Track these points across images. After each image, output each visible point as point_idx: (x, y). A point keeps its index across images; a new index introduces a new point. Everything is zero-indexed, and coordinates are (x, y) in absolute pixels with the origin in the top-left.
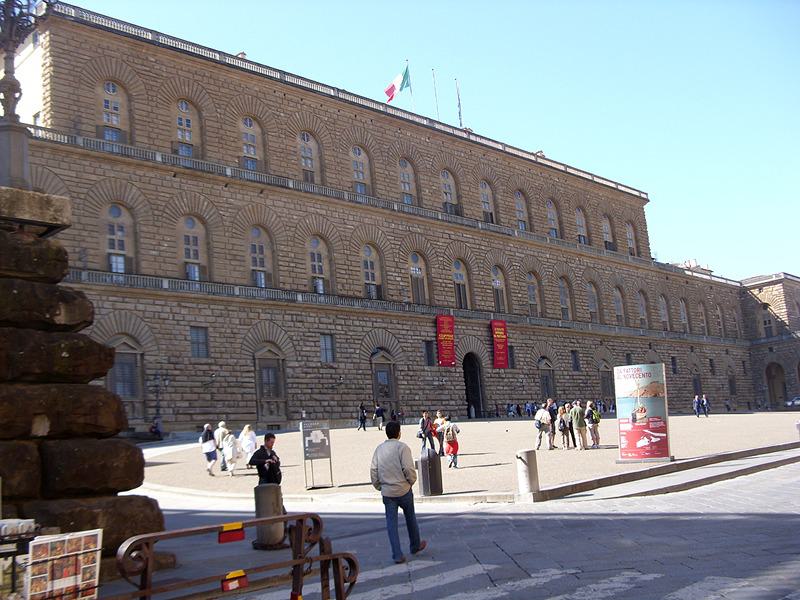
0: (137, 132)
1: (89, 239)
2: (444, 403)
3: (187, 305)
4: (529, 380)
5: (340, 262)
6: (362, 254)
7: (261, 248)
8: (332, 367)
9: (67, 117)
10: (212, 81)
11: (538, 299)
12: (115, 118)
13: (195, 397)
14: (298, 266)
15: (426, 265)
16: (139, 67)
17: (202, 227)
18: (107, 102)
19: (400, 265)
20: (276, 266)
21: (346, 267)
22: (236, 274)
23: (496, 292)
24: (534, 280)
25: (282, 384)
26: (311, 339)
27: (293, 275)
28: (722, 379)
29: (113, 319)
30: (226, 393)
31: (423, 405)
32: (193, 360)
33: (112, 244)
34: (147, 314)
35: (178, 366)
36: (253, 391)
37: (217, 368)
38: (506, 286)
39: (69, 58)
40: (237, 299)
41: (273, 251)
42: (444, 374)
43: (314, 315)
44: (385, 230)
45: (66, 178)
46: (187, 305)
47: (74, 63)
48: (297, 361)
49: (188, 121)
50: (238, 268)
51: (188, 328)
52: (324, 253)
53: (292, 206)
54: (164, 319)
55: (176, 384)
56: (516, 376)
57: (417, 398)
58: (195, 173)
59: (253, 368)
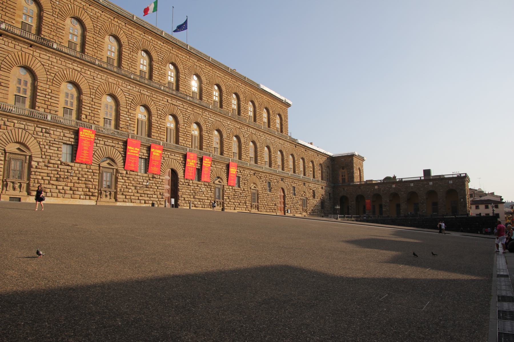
2: (149, 196)
4: (207, 189)
5: (86, 101)
8: (69, 165)
14: (53, 98)
21: (91, 105)
26: (54, 145)
27: (47, 103)
31: (134, 196)
42: (151, 179)
43: (61, 131)
48: (42, 158)
52: (75, 94)
53: (55, 61)
57: (130, 191)
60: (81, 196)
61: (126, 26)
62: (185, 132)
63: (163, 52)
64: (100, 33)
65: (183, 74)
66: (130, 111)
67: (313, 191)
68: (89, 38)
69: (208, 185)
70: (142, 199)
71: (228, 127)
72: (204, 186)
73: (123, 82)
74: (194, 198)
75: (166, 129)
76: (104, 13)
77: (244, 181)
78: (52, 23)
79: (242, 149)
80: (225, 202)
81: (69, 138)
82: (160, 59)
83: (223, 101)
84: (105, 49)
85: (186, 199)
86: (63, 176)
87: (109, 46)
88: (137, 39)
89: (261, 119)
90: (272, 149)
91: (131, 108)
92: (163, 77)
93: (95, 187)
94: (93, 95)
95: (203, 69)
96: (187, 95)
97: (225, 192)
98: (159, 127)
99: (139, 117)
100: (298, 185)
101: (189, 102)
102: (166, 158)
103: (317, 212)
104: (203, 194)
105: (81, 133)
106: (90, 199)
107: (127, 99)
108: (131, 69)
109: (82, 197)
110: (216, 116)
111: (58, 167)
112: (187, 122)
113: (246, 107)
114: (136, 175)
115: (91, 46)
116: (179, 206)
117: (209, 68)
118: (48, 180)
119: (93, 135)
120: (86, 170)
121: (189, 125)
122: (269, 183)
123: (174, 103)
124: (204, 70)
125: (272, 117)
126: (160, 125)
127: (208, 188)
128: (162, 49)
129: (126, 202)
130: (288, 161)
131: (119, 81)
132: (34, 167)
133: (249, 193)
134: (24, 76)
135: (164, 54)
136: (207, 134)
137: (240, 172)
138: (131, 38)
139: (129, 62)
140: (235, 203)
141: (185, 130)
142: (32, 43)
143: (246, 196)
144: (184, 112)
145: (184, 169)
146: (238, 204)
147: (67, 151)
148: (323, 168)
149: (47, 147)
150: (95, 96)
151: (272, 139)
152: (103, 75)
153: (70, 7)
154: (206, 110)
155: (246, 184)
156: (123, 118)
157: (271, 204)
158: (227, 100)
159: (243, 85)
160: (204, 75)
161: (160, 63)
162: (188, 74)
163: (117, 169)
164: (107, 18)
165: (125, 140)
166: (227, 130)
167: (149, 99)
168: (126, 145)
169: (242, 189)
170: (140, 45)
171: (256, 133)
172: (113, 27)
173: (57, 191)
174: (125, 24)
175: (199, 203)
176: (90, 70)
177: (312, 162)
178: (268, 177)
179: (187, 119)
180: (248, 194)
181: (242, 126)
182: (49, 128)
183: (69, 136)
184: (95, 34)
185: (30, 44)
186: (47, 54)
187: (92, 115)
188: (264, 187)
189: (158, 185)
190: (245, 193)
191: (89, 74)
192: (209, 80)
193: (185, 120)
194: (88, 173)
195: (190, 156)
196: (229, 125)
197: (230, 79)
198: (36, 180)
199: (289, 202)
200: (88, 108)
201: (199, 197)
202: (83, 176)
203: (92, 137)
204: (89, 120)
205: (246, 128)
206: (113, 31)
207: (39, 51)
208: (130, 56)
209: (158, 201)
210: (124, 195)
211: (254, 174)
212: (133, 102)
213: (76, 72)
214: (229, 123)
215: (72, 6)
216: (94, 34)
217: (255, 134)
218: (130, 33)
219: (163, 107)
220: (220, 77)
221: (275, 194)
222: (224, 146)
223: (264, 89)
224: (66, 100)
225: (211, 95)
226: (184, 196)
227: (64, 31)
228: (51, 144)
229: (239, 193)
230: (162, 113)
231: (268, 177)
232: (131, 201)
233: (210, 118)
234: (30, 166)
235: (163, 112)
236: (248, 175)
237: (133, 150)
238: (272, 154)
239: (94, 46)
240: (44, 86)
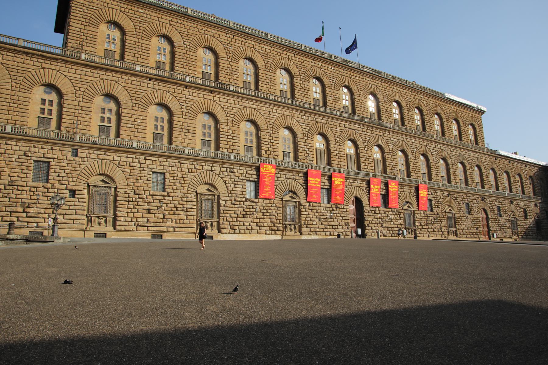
1: (84, 116)
2: (334, 227)
4: (396, 216)
8: (253, 202)
10: (182, 26)
14: (234, 138)
16: (132, 15)
18: (109, 35)
21: (269, 141)
22: (187, 141)
26: (239, 183)
27: (229, 143)
30: (174, 214)
31: (318, 228)
33: (103, 119)
39: (84, 8)
42: (335, 209)
44: (298, 119)
45: (72, 78)
47: (86, 11)
48: (228, 196)
50: (190, 138)
52: (254, 131)
53: (233, 102)
56: (387, 213)
57: (314, 223)
59: (195, 200)
60: (267, 231)
61: (295, 57)
62: (366, 157)
63: (335, 76)
64: (271, 69)
65: (358, 95)
66: (308, 141)
67: (525, 210)
68: (262, 75)
69: (396, 212)
70: (327, 231)
71: (413, 146)
72: (392, 213)
73: (298, 113)
74: (382, 226)
75: (345, 156)
76: (273, 49)
77: (437, 204)
78: (227, 67)
79: (432, 168)
80: (417, 230)
81: (252, 174)
82: (332, 83)
83: (405, 118)
84: (278, 83)
85: (374, 228)
86: (248, 213)
87: (281, 79)
88: (307, 68)
89: (450, 132)
90: (467, 165)
91: (309, 138)
92: (338, 101)
93: (280, 221)
94: (270, 130)
95: (378, 87)
96: (364, 117)
97: (416, 218)
98: (338, 155)
99: (317, 146)
100: (503, 204)
101: (367, 124)
102: (348, 186)
103: (532, 235)
104: (392, 221)
105: (262, 169)
106: (275, 234)
107: (304, 129)
108: (305, 99)
109: (268, 232)
110: (398, 136)
111: (244, 203)
112: (367, 146)
113: (432, 121)
114: (319, 206)
115: (264, 83)
116: (367, 236)
117: (386, 85)
118: (236, 217)
119: (274, 170)
120: (270, 205)
121: (370, 148)
122: (467, 204)
123: (352, 127)
124: (380, 88)
125: (464, 128)
126: (339, 152)
127: (397, 214)
128: (333, 73)
129: (311, 235)
130: (489, 177)
131: (294, 112)
132: (222, 205)
133: (444, 217)
134: (207, 121)
135: (336, 78)
136: (390, 156)
137: (432, 194)
138: (301, 68)
139: (302, 92)
140: (429, 230)
141: (366, 155)
142: (212, 89)
143: (441, 221)
144: (363, 135)
145: (368, 196)
146: (432, 230)
147: (251, 188)
148: (535, 180)
149: (232, 186)
150: (272, 130)
151: (466, 154)
152: (277, 109)
153: (242, 50)
154: (387, 130)
155: (440, 207)
156: (301, 149)
157: (472, 229)
158: (408, 116)
159: (425, 98)
160: (380, 93)
161: (333, 88)
162: (363, 95)
163: (299, 202)
164: (276, 53)
165: (305, 171)
166: (412, 149)
167: (326, 126)
168: (306, 176)
169: (436, 213)
170: (311, 73)
171: (446, 149)
172: (283, 60)
173: (245, 227)
174: (294, 54)
175: (388, 232)
176: (265, 106)
177: (519, 175)
178: (465, 197)
179: (367, 142)
180: (443, 219)
181: (428, 143)
182: (233, 167)
183: (252, 173)
184: (267, 70)
185: (211, 90)
186: (226, 97)
187: (271, 149)
188: (462, 209)
189: (342, 215)
190: (439, 217)
191: (265, 110)
192: (386, 97)
193: (365, 144)
194: (272, 208)
195: (374, 182)
196: (414, 144)
197: (410, 93)
198: (225, 218)
199: (493, 225)
200: (267, 143)
201: (388, 226)
202: (267, 211)
203: (272, 172)
204: (269, 155)
205: (434, 144)
206: (283, 64)
207: (218, 96)
208: (302, 85)
209: (344, 231)
210: (309, 228)
211: (448, 195)
212: (309, 131)
213: (253, 110)
214: (413, 141)
215: (244, 47)
216: (266, 70)
217: (445, 150)
218: (300, 63)
219: (341, 132)
220: (398, 93)
221: (476, 216)
222: (411, 167)
223: (451, 98)
224: (246, 139)
225: (390, 113)
226: (371, 225)
227: (238, 72)
228: (236, 183)
229: (433, 218)
230: (340, 140)
231: (465, 197)
232: (316, 233)
233: (391, 139)
234: (219, 205)
235: (341, 138)
236: (442, 197)
237: (313, 181)
238: (468, 171)
239: (267, 81)
240: (226, 128)
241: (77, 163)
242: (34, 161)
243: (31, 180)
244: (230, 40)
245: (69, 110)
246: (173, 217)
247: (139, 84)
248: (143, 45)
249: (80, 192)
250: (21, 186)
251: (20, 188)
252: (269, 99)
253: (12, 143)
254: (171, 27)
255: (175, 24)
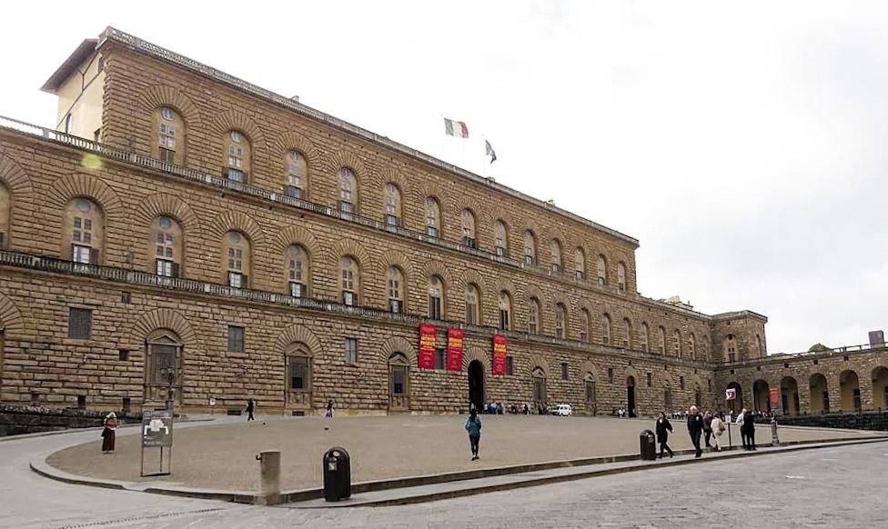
0: (190, 155)
3: (227, 307)
6: (388, 274)
7: (299, 264)
8: (353, 366)
9: (123, 135)
11: (537, 320)
12: (170, 141)
13: (229, 385)
15: (443, 287)
17: (245, 241)
18: (163, 126)
19: (420, 286)
20: (311, 279)
22: (273, 284)
23: (503, 313)
24: (535, 305)
25: (309, 377)
28: (689, 393)
29: (156, 315)
32: (229, 354)
33: (160, 250)
34: (189, 313)
35: (214, 359)
36: (282, 382)
37: (251, 362)
38: (511, 308)
40: (273, 305)
41: (309, 268)
44: (410, 255)
46: (227, 307)
47: (134, 89)
49: (239, 150)
50: (275, 279)
51: (227, 327)
52: (355, 271)
53: (329, 230)
54: (204, 318)
55: (211, 373)
58: (240, 197)
59: (283, 364)
109: (371, 406)
142: (304, 212)
149: (328, 345)
185: (300, 213)
189: (459, 384)
200: (370, 288)
217: (587, 298)
241: (131, 311)
242: (71, 308)
243: (66, 335)
244: (325, 140)
245: (117, 236)
246: (255, 386)
247: (208, 201)
248: (212, 144)
249: (136, 353)
250: (54, 344)
251: (52, 347)
252: (374, 228)
253: (40, 282)
254: (248, 119)
255: (252, 113)
